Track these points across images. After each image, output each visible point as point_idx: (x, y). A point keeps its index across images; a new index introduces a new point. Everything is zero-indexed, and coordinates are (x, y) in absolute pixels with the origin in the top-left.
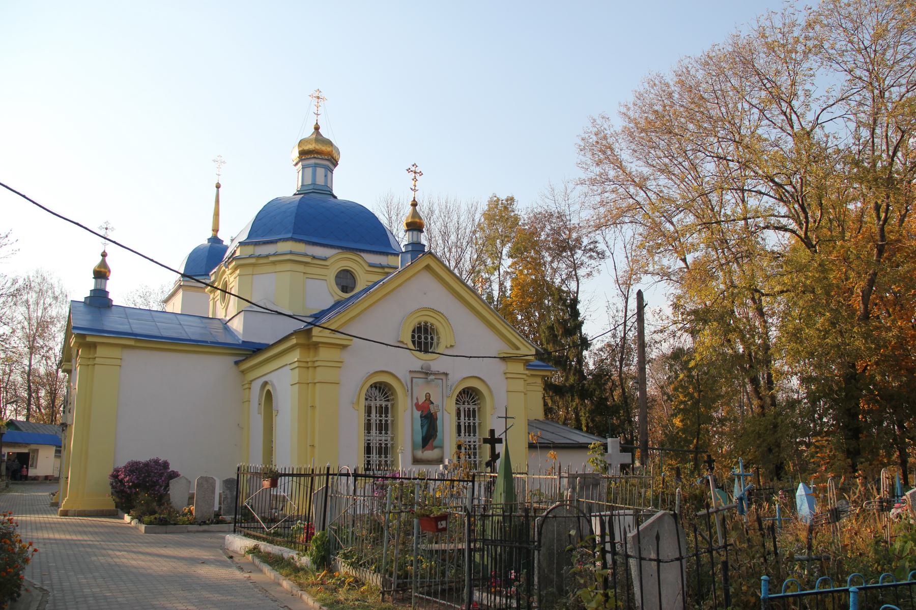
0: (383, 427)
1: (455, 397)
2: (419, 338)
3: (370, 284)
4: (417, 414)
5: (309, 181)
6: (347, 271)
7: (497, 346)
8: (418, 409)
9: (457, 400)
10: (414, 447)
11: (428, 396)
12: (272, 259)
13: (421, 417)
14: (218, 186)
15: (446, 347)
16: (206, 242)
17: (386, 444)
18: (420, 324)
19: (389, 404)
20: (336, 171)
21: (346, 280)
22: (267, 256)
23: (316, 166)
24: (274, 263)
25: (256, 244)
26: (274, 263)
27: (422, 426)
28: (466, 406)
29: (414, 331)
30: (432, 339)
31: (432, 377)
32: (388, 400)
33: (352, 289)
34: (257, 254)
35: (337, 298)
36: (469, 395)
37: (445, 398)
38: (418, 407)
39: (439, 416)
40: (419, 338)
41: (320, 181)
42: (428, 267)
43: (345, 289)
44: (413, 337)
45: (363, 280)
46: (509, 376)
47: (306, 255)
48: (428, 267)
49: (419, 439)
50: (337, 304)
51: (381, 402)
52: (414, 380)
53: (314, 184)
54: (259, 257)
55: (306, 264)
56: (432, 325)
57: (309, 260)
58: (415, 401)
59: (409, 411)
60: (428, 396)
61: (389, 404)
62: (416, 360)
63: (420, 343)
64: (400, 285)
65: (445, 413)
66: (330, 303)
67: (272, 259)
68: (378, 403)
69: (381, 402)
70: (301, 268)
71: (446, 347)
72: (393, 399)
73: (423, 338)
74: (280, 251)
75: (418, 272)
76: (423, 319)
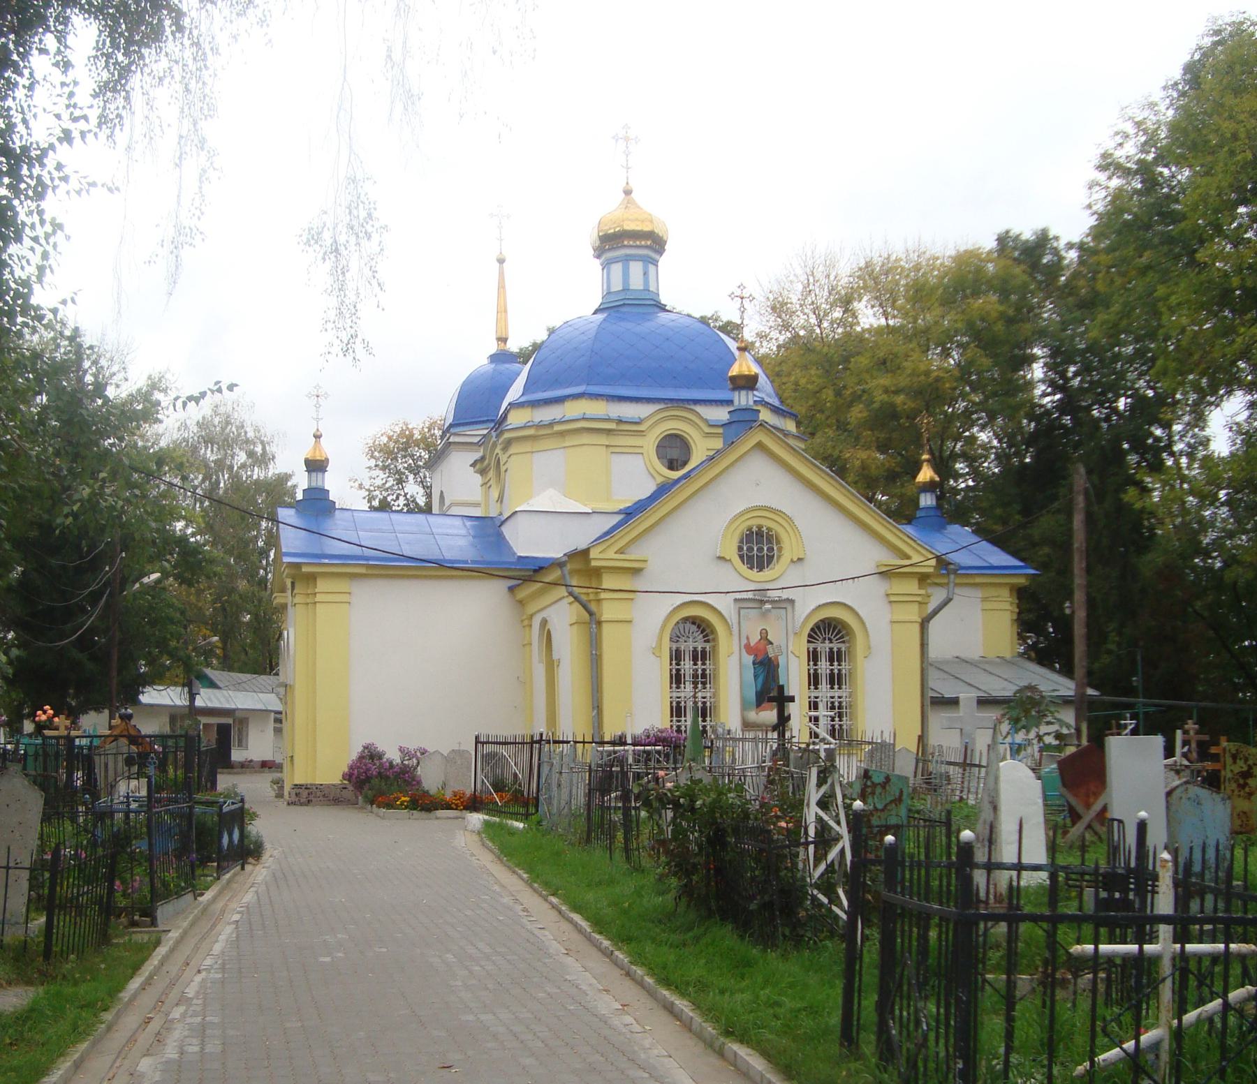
0: (702, 679)
1: (807, 630)
2: (750, 549)
3: (711, 453)
4: (749, 659)
5: (617, 286)
6: (676, 436)
7: (871, 556)
8: (749, 653)
9: (810, 636)
10: (744, 706)
11: (764, 635)
12: (557, 428)
13: (754, 663)
14: (501, 261)
15: (792, 561)
16: (485, 361)
17: (704, 703)
18: (750, 529)
19: (708, 646)
20: (663, 261)
21: (674, 452)
22: (551, 424)
23: (626, 260)
24: (562, 434)
25: (535, 404)
26: (562, 434)
27: (756, 677)
28: (827, 645)
29: (741, 541)
30: (771, 549)
31: (768, 606)
32: (707, 641)
33: (685, 463)
34: (537, 420)
35: (660, 480)
36: (831, 633)
37: (791, 638)
38: (749, 649)
39: (781, 661)
40: (750, 549)
41: (636, 283)
42: (760, 446)
43: (672, 466)
44: (740, 549)
45: (701, 448)
46: (893, 599)
47: (608, 420)
48: (760, 446)
49: (752, 695)
50: (663, 489)
51: (694, 642)
52: (742, 612)
53: (626, 289)
54: (539, 426)
55: (609, 432)
56: (769, 529)
57: (613, 426)
58: (744, 641)
59: (735, 658)
60: (764, 635)
61: (708, 646)
62: (742, 580)
63: (750, 558)
64: (732, 464)
65: (791, 656)
66: (648, 489)
67: (557, 428)
68: (690, 645)
69: (694, 642)
70: (603, 440)
71: (792, 561)
72: (714, 640)
73: (758, 547)
74: (569, 416)
75: (746, 453)
76: (754, 523)
